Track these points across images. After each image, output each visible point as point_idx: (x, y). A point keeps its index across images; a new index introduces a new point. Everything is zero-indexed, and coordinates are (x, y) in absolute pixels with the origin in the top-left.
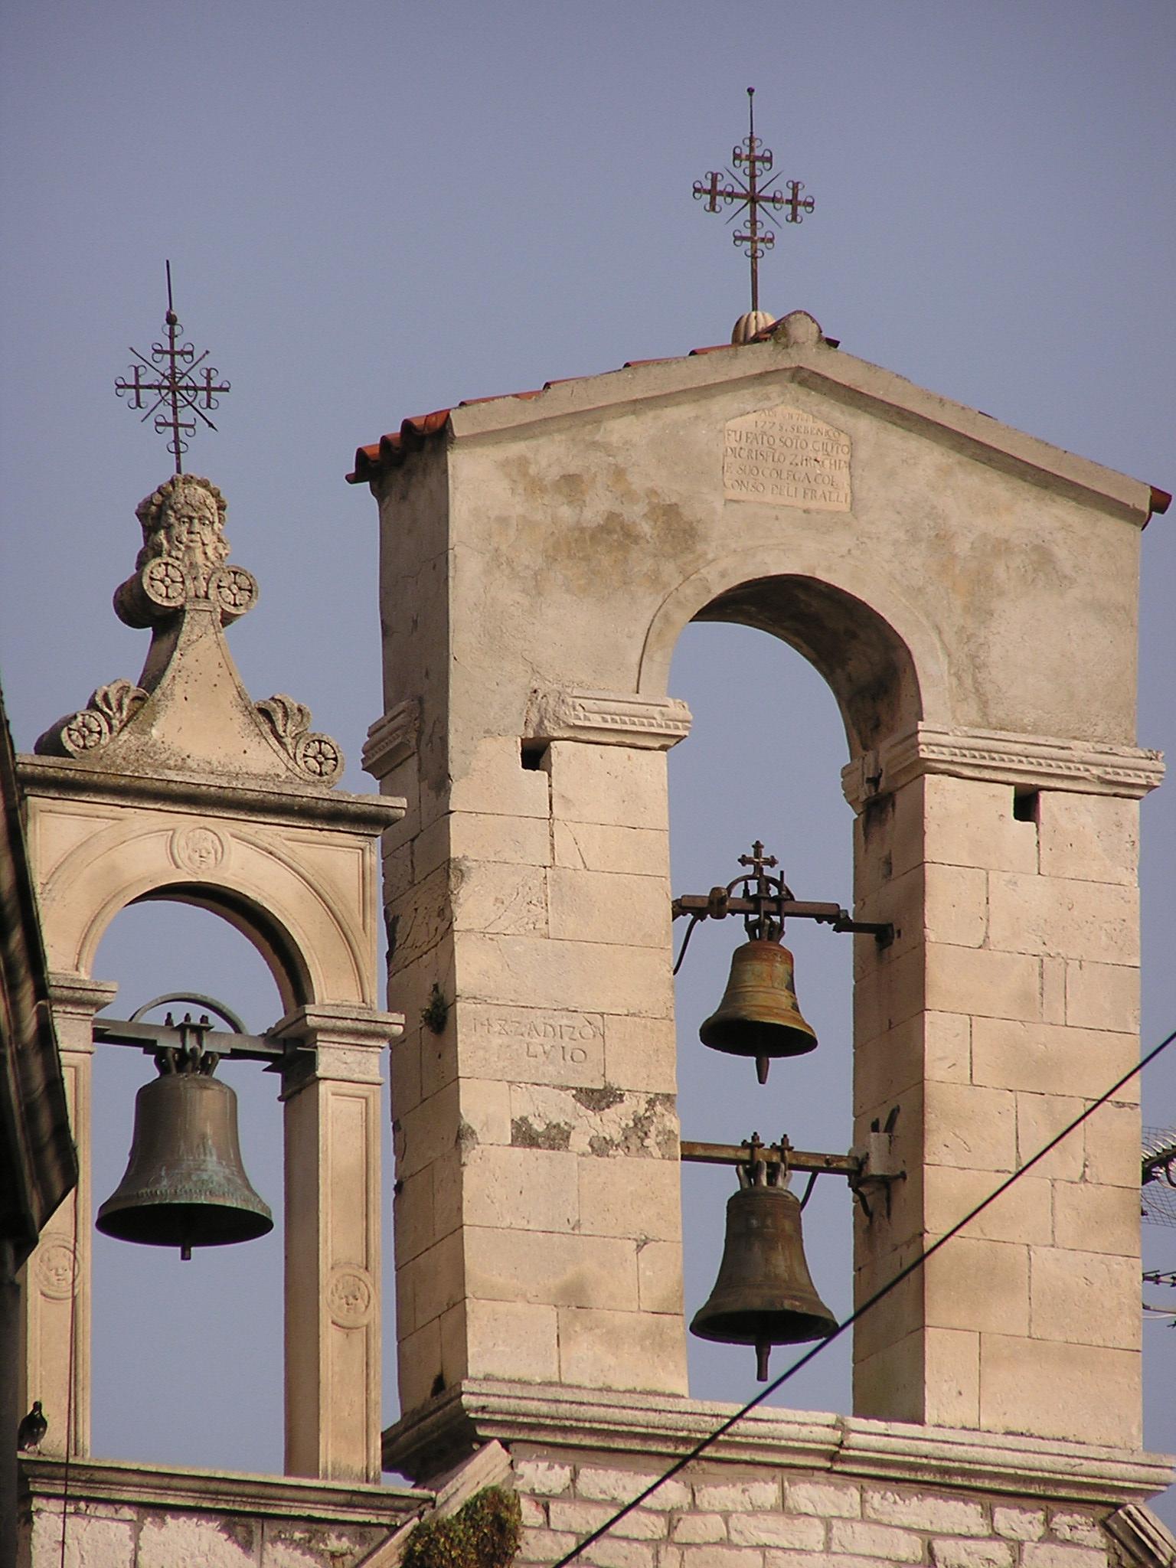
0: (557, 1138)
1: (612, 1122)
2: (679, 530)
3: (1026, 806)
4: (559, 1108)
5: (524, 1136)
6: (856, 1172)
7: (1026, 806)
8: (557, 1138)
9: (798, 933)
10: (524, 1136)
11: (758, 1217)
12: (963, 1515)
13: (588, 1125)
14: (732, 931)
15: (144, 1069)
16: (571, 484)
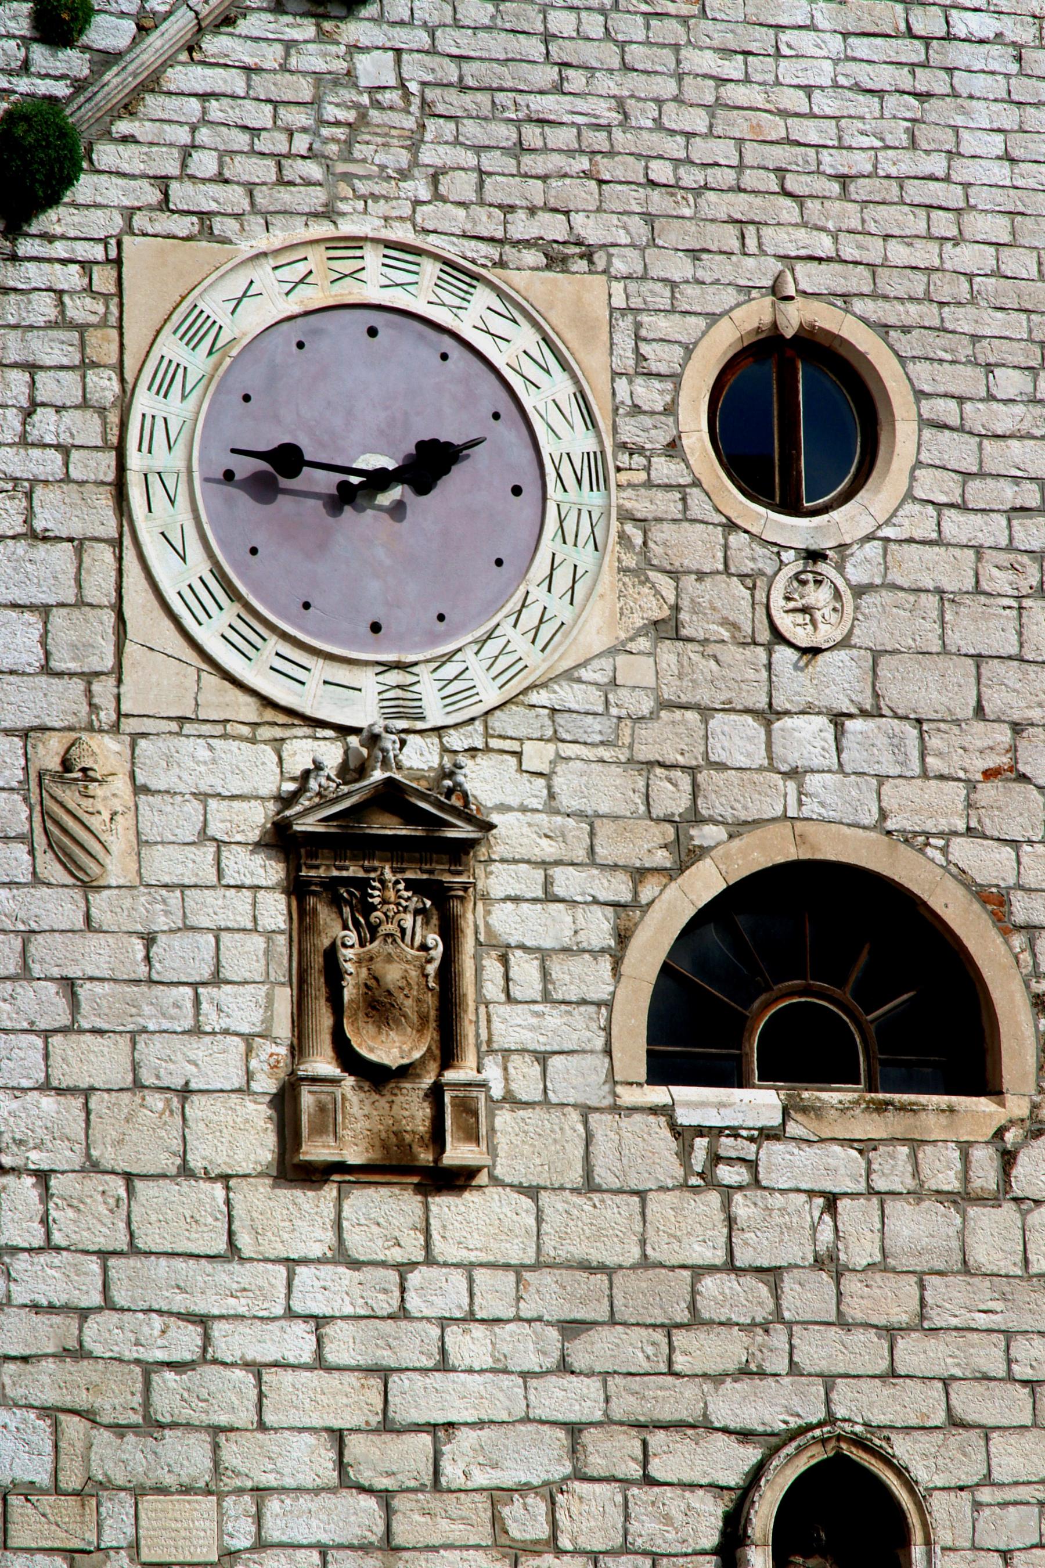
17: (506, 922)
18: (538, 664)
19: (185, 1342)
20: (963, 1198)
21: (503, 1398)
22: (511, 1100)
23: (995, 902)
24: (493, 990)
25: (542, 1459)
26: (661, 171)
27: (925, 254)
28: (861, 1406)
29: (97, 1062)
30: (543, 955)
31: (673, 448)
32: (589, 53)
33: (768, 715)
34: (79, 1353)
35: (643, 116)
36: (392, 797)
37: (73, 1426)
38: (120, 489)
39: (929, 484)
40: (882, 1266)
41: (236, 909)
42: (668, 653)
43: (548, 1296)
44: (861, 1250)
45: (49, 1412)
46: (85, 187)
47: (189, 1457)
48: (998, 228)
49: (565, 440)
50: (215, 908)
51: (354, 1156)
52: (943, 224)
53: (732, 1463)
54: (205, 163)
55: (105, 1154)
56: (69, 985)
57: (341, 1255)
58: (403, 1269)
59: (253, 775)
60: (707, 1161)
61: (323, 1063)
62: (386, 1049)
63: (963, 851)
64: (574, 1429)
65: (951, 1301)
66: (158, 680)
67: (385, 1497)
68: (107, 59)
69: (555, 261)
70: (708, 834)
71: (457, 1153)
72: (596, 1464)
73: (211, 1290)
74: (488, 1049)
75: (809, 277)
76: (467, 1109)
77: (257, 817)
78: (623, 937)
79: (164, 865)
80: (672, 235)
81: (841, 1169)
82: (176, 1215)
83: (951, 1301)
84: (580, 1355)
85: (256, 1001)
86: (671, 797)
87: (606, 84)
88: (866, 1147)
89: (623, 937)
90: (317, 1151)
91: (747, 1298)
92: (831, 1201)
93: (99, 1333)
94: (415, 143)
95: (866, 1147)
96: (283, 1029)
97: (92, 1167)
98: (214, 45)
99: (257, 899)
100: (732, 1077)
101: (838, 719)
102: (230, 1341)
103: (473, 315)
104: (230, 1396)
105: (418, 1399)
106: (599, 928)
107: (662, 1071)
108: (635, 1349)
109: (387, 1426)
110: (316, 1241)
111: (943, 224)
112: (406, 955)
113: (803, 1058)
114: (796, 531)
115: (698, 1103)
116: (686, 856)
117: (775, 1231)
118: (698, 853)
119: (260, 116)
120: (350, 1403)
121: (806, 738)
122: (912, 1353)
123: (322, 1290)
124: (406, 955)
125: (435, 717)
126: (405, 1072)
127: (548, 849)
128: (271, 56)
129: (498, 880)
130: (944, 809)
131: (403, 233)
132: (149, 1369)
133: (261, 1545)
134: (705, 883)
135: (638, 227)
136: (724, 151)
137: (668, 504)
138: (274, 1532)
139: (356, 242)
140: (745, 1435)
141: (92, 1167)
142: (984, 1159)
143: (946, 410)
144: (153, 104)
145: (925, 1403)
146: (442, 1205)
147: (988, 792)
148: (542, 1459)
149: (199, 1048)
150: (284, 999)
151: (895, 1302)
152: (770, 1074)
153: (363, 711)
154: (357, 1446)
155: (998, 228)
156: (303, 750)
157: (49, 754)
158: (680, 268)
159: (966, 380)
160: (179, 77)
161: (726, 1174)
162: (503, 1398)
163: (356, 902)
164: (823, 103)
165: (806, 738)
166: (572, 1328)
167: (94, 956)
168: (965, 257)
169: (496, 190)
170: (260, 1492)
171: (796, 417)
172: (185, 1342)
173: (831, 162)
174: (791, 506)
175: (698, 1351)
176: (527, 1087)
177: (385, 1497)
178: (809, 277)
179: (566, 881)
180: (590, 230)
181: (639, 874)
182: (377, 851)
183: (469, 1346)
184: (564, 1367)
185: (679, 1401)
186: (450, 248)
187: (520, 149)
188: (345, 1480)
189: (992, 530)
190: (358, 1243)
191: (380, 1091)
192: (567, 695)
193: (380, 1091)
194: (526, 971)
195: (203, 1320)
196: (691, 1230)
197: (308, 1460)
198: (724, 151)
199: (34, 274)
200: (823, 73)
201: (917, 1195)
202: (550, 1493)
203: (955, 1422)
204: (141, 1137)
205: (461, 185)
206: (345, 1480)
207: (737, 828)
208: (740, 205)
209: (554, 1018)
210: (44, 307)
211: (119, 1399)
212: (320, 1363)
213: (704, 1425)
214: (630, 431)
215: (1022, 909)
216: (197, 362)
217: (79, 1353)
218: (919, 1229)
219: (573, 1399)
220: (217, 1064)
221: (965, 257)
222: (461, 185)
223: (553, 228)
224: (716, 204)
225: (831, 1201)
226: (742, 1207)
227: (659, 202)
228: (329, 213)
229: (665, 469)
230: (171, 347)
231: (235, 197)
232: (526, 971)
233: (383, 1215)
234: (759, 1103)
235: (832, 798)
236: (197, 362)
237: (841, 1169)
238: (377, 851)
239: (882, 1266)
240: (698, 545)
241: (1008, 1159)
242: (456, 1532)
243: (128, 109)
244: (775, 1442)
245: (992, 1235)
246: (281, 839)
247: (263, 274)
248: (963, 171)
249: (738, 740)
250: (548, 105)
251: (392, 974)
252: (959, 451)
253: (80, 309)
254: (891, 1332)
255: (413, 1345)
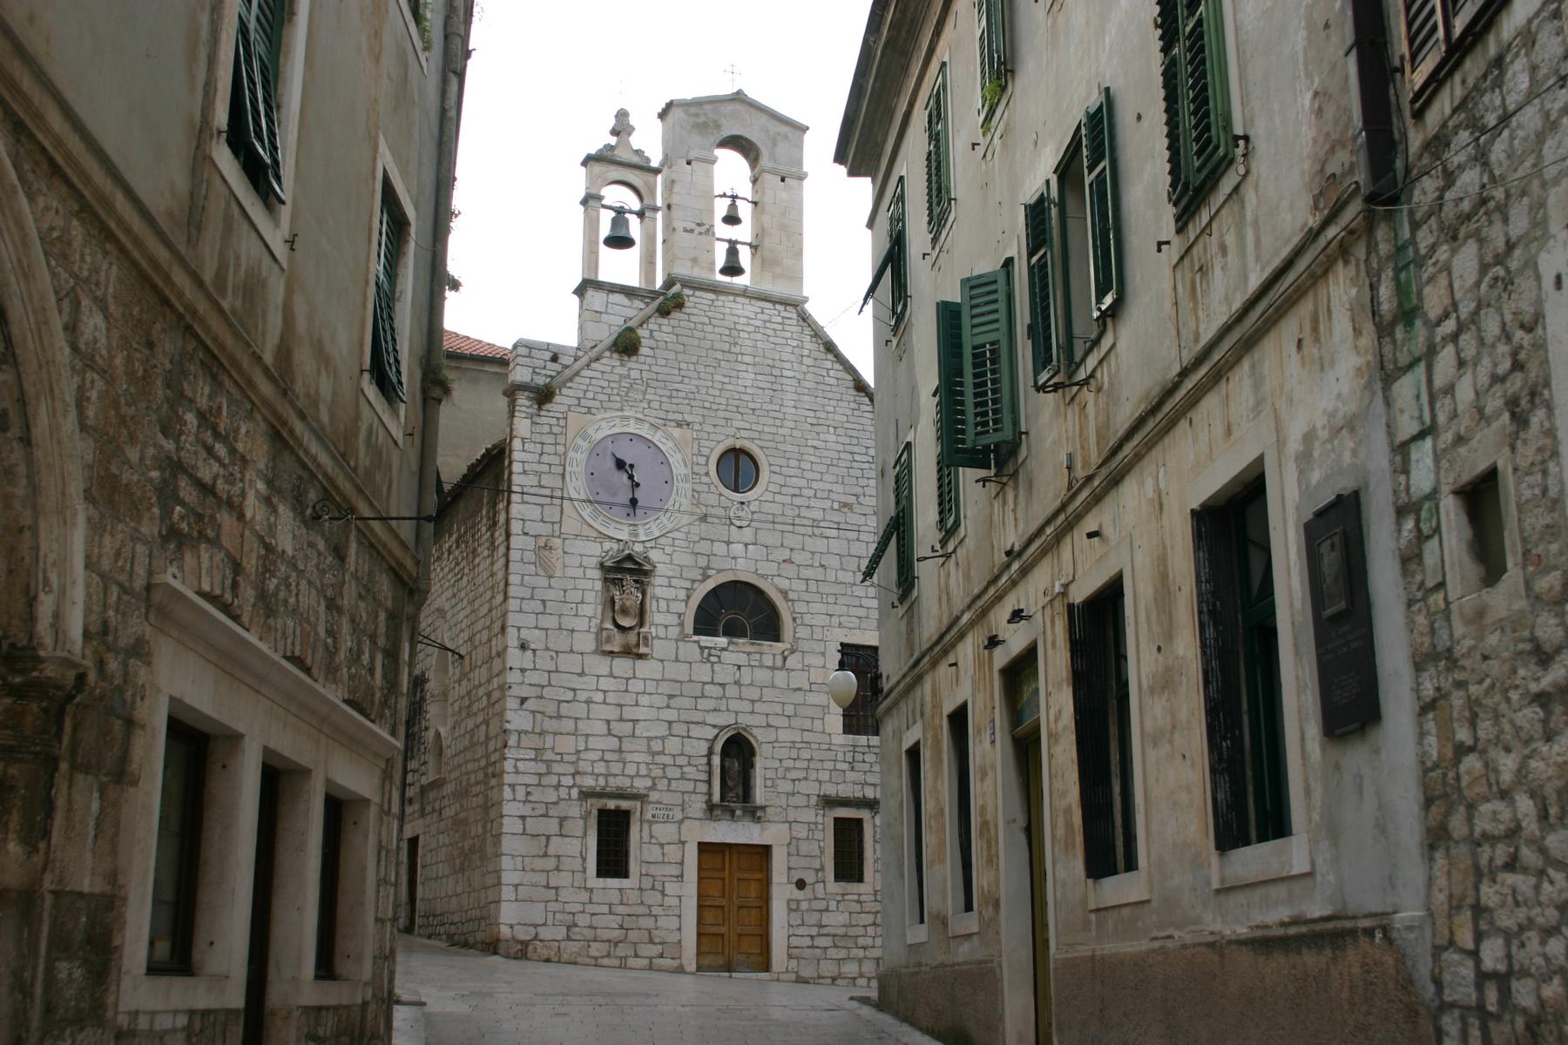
0: (692, 231)
1: (703, 229)
2: (718, 127)
3: (783, 180)
4: (693, 226)
5: (685, 230)
6: (750, 245)
7: (783, 180)
8: (692, 231)
9: (738, 202)
10: (685, 230)
11: (732, 252)
12: (769, 305)
13: (698, 229)
14: (728, 201)
15: (613, 214)
16: (697, 115)
17: (658, 591)
18: (670, 526)
19: (569, 695)
20: (773, 668)
21: (652, 714)
22: (658, 637)
23: (784, 593)
24: (654, 608)
25: (662, 730)
26: (707, 405)
27: (773, 430)
28: (744, 720)
29: (550, 622)
30: (668, 600)
31: (707, 474)
32: (690, 374)
33: (728, 543)
34: (541, 697)
35: (703, 391)
36: (630, 558)
37: (539, 716)
38: (563, 475)
39: (772, 488)
40: (751, 684)
41: (589, 584)
42: (703, 525)
43: (665, 688)
44: (746, 680)
45: (533, 712)
46: (557, 399)
47: (568, 725)
48: (792, 425)
49: (679, 469)
50: (583, 584)
51: (616, 649)
52: (778, 422)
53: (710, 733)
54: (590, 395)
55: (550, 645)
56: (544, 602)
57: (611, 675)
58: (628, 679)
59: (594, 552)
60: (707, 655)
61: (609, 625)
62: (626, 622)
63: (776, 580)
64: (670, 723)
65: (769, 694)
66: (570, 526)
67: (620, 738)
68: (566, 367)
69: (679, 425)
70: (711, 572)
71: (643, 650)
72: (675, 732)
73: (576, 682)
74: (652, 624)
75: (744, 434)
76: (646, 638)
77: (594, 561)
78: (688, 597)
79: (570, 572)
80: (709, 421)
81: (742, 659)
82: (566, 662)
83: (769, 694)
84: (673, 703)
85: (592, 608)
86: (703, 562)
87: (695, 382)
88: (749, 654)
89: (688, 597)
90: (608, 648)
91: (717, 691)
92: (739, 667)
93: (546, 692)
94: (645, 393)
95: (749, 654)
96: (599, 616)
97: (547, 649)
98: (593, 365)
99: (593, 583)
100: (714, 634)
101: (746, 545)
102: (582, 696)
103: (657, 438)
104: (580, 711)
105: (629, 713)
106: (682, 595)
107: (697, 632)
108: (687, 703)
109: (621, 720)
110: (605, 671)
111: (778, 422)
112: (632, 598)
113: (732, 631)
114: (738, 497)
115: (706, 640)
116: (706, 577)
117: (725, 674)
118: (709, 577)
119: (605, 384)
120: (612, 713)
121: (738, 549)
122: (758, 707)
123: (606, 684)
124: (632, 598)
125: (643, 538)
126: (631, 628)
127: (670, 574)
128: (608, 369)
129: (657, 581)
130: (772, 568)
131: (640, 416)
132: (560, 702)
133: (587, 749)
134: (710, 585)
135: (700, 419)
136: (724, 401)
137: (705, 488)
138: (591, 746)
139: (627, 418)
140: (714, 726)
141: (547, 649)
142: (779, 659)
143: (777, 469)
144: (577, 379)
145: (762, 720)
146: (639, 663)
147: (784, 565)
148: (662, 730)
149: (577, 620)
150: (600, 608)
151: (754, 693)
152: (725, 634)
153: (624, 536)
154: (613, 725)
155: (792, 425)
156: (607, 545)
157: (542, 542)
158: (711, 429)
159: (783, 462)
160: (584, 373)
161: (713, 659)
162: (652, 714)
163: (618, 583)
164: (749, 390)
165: (738, 549)
166: (671, 697)
167: (551, 595)
168: (782, 431)
169: (665, 406)
170: (587, 735)
171: (738, 467)
172: (569, 695)
173: (751, 405)
174: (736, 490)
175: (702, 704)
176: (662, 635)
177: (620, 738)
178: (744, 434)
179: (675, 582)
180: (689, 418)
181: (693, 581)
182: (626, 571)
183: (644, 700)
184: (668, 707)
185: (698, 717)
186: (653, 420)
187: (671, 397)
188: (610, 733)
189: (788, 500)
190: (616, 673)
191: (626, 633)
192: (676, 535)
193: (626, 633)
194: (663, 604)
195: (574, 690)
196: (703, 672)
197: (601, 728)
198: (724, 401)
199: (544, 420)
200: (749, 383)
201: (761, 666)
202: (663, 738)
203: (769, 726)
204: (561, 642)
205: (655, 405)
206: (610, 733)
207: (719, 571)
208: (727, 415)
209: (669, 617)
210: (546, 429)
211: (551, 709)
212: (604, 702)
213: (704, 723)
214: (696, 469)
215: (791, 595)
216: (585, 445)
217: (541, 697)
218: (761, 675)
219: (671, 715)
220: (581, 624)
221: (782, 431)
222: (655, 405)
223: (679, 417)
224: (720, 414)
225: (739, 667)
226: (716, 667)
227: (706, 412)
228: (621, 410)
229: (705, 479)
230: (579, 441)
231: (597, 404)
232: (663, 604)
233: (623, 665)
234: (722, 641)
235: (742, 563)
236: (585, 445)
237: (742, 659)
238: (626, 571)
239: (751, 684)
240: (712, 499)
241: (785, 659)
242: (638, 748)
243: (571, 380)
244: (722, 728)
245: (780, 678)
246: (602, 566)
247: (603, 424)
248: (784, 410)
249: (720, 548)
250: (680, 386)
251: (628, 603)
252: (780, 479)
253: (556, 430)
254: (753, 701)
255: (629, 699)
